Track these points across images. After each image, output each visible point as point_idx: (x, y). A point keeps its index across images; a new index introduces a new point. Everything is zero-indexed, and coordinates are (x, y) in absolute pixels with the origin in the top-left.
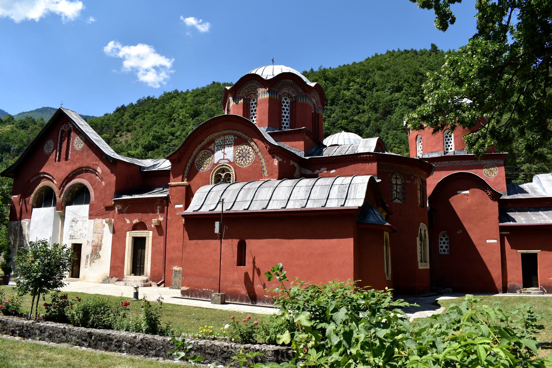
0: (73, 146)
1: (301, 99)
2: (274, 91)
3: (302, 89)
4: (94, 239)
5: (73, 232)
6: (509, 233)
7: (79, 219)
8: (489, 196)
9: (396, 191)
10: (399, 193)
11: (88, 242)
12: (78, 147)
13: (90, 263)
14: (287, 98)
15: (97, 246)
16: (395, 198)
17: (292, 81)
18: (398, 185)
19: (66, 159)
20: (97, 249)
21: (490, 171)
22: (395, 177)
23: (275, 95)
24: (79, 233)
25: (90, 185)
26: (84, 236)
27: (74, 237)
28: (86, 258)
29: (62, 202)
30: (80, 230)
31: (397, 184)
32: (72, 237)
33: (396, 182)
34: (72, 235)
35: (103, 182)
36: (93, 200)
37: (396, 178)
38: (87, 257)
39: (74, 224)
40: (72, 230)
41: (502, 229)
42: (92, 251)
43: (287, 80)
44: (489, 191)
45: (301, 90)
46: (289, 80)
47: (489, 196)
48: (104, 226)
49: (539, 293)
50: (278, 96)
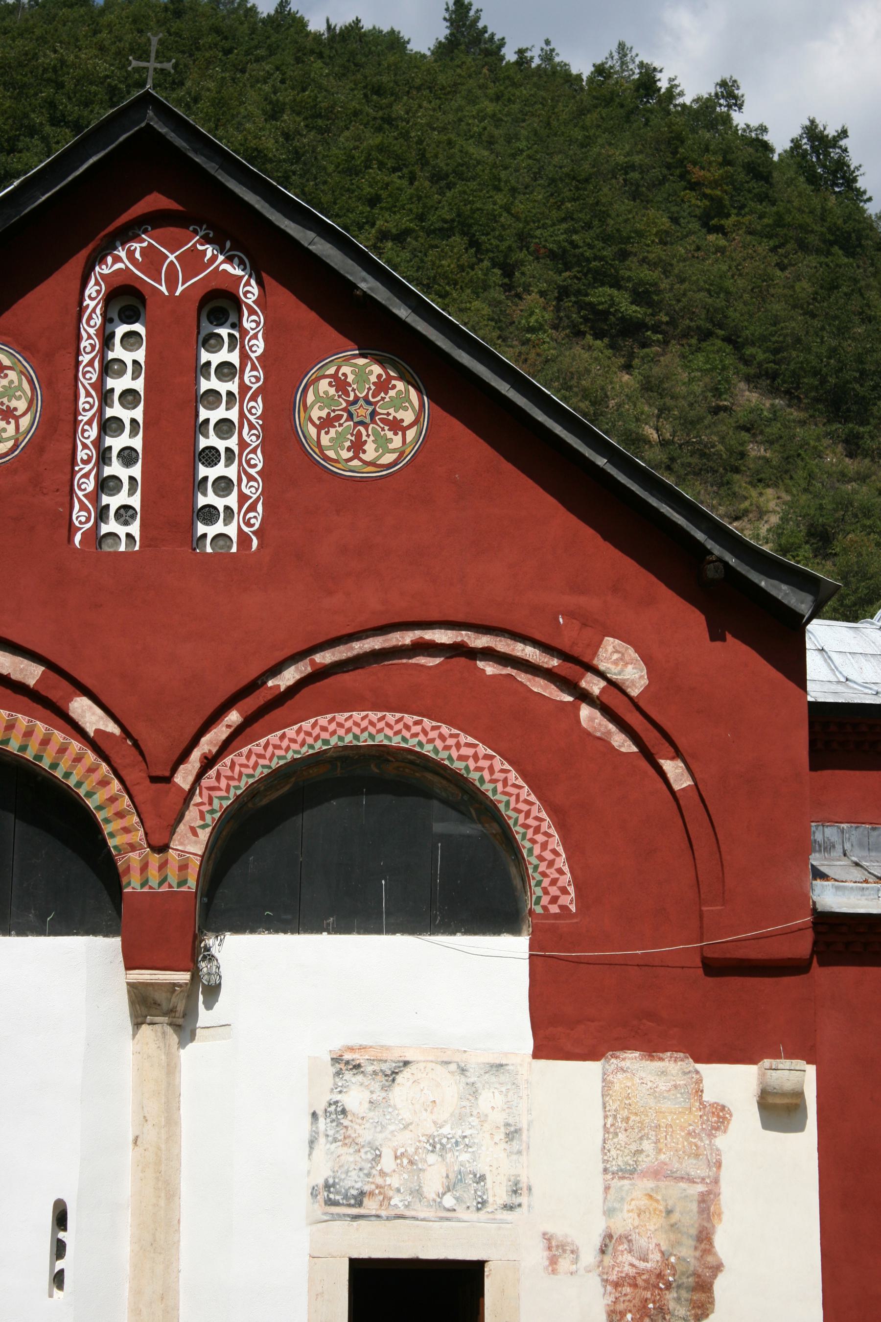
4: (624, 1222)
5: (348, 1156)
12: (358, 446)
25: (513, 776)
26: (498, 1194)
27: (370, 1206)
29: (196, 892)
30: (435, 1145)
34: (353, 1182)
35: (673, 768)
36: (569, 900)
40: (348, 1141)
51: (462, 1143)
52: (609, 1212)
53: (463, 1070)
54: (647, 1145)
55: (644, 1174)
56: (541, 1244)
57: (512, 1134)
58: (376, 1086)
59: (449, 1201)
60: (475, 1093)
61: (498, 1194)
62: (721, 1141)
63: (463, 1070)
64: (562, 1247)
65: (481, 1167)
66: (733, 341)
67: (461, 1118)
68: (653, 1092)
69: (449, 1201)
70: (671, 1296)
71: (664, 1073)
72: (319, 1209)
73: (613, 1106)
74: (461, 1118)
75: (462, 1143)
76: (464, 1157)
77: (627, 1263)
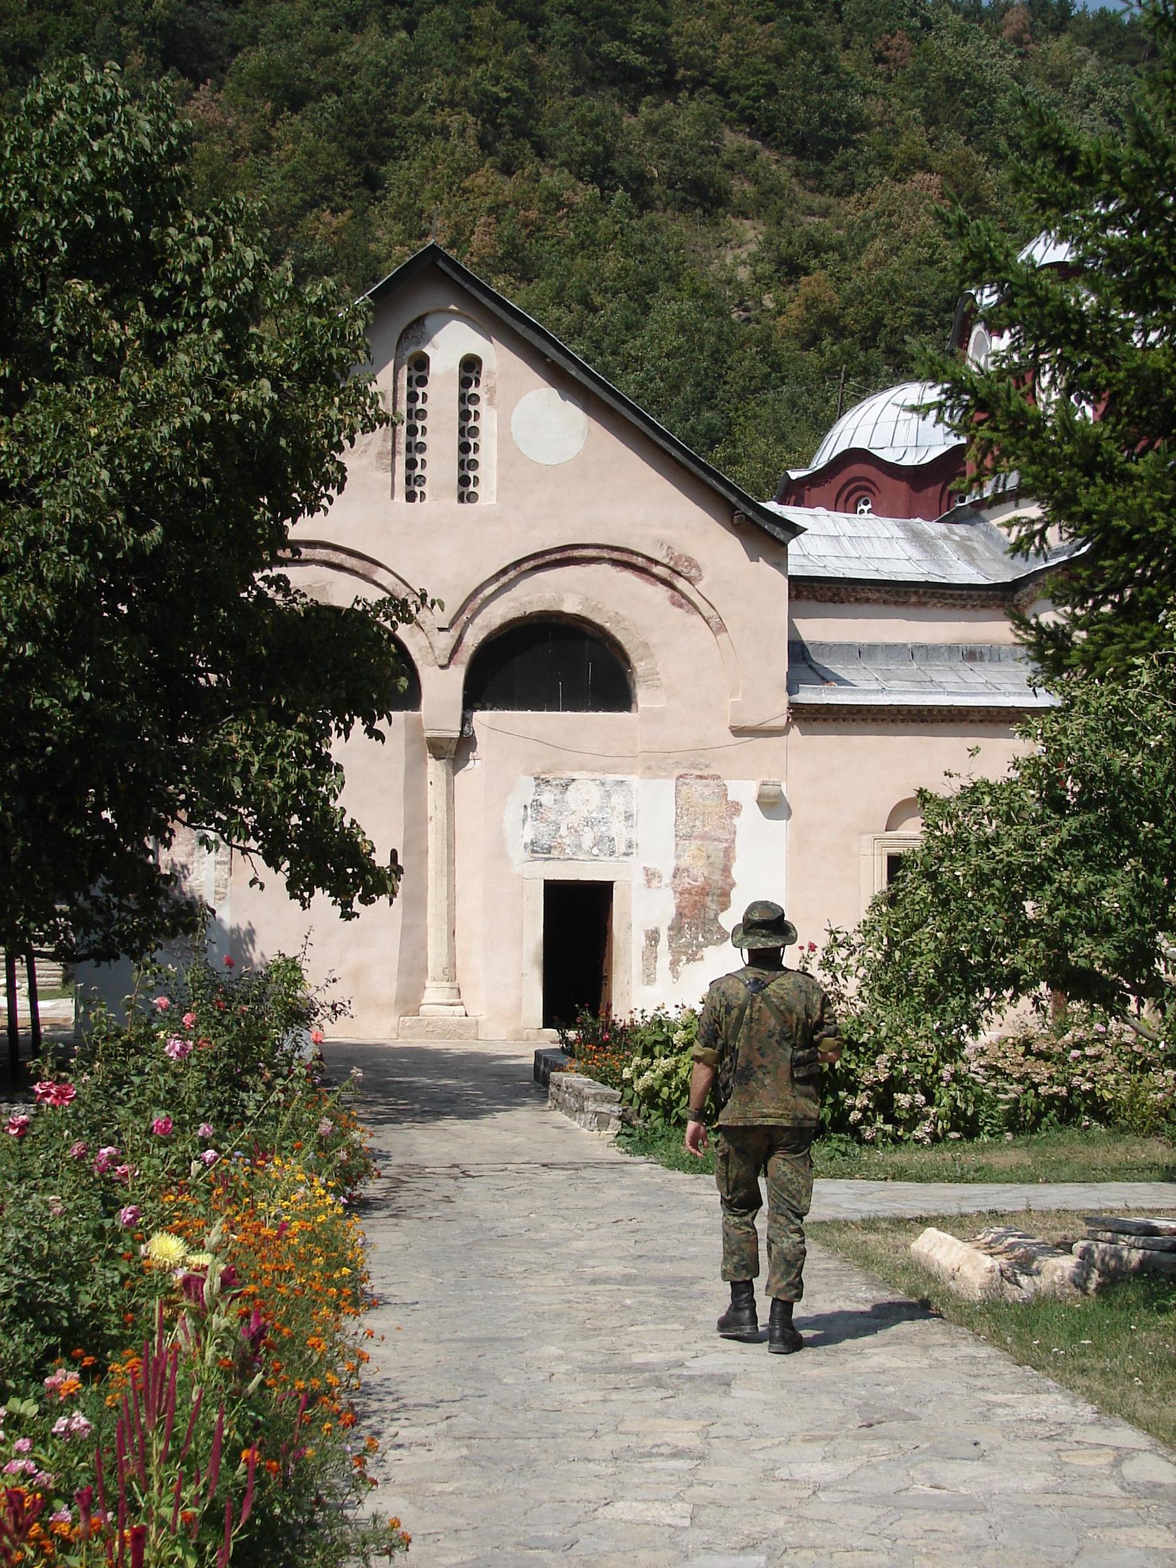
0: (506, 439)
4: (686, 862)
5: (543, 827)
7: (575, 775)
11: (651, 876)
13: (674, 963)
15: (704, 892)
19: (466, 488)
20: (704, 906)
24: (587, 840)
26: (621, 848)
27: (555, 853)
28: (638, 941)
30: (589, 823)
32: (539, 850)
34: (546, 841)
38: (653, 937)
39: (547, 798)
40: (542, 820)
42: (680, 914)
48: (735, 808)
51: (603, 821)
52: (678, 857)
53: (603, 784)
54: (698, 823)
55: (697, 837)
56: (643, 873)
57: (628, 817)
58: (557, 791)
59: (595, 851)
60: (609, 796)
61: (621, 848)
62: (736, 821)
63: (603, 784)
64: (654, 874)
65: (612, 834)
66: (721, 89)
67: (602, 809)
68: (701, 796)
69: (595, 851)
70: (709, 899)
71: (707, 786)
72: (527, 855)
73: (680, 803)
74: (602, 809)
75: (603, 821)
76: (603, 829)
77: (686, 882)
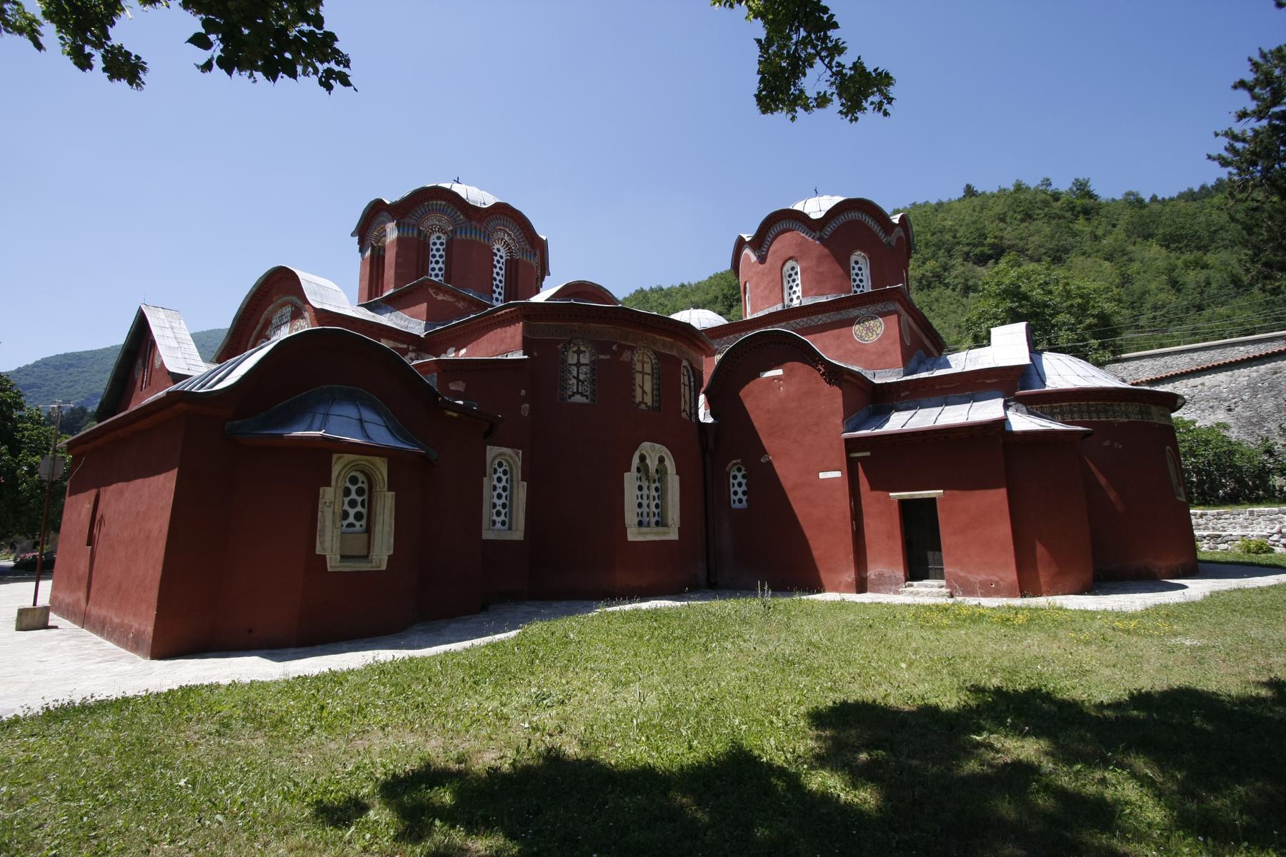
1: (461, 233)
2: (409, 224)
3: (464, 215)
6: (868, 454)
8: (822, 375)
9: (577, 378)
10: (583, 382)
14: (441, 235)
16: (574, 394)
17: (444, 203)
18: (583, 365)
21: (868, 329)
22: (575, 349)
23: (410, 232)
31: (578, 365)
33: (578, 359)
37: (579, 352)
41: (851, 445)
43: (435, 202)
44: (821, 365)
45: (462, 217)
46: (439, 202)
47: (822, 375)
49: (940, 595)
50: (416, 232)
